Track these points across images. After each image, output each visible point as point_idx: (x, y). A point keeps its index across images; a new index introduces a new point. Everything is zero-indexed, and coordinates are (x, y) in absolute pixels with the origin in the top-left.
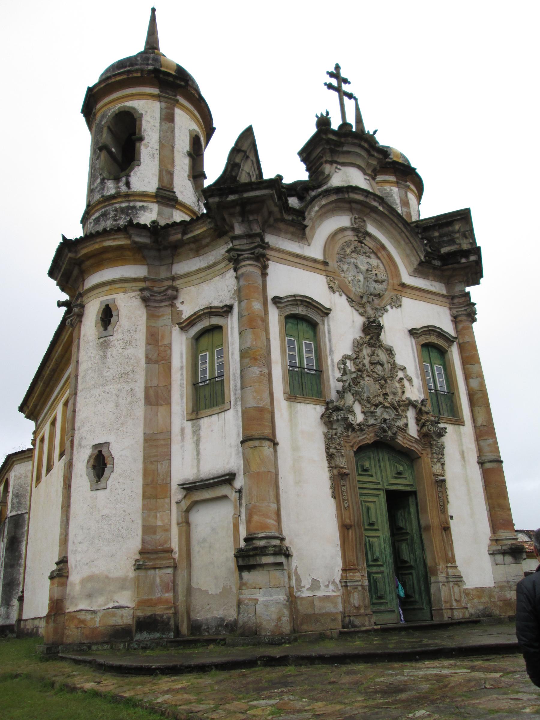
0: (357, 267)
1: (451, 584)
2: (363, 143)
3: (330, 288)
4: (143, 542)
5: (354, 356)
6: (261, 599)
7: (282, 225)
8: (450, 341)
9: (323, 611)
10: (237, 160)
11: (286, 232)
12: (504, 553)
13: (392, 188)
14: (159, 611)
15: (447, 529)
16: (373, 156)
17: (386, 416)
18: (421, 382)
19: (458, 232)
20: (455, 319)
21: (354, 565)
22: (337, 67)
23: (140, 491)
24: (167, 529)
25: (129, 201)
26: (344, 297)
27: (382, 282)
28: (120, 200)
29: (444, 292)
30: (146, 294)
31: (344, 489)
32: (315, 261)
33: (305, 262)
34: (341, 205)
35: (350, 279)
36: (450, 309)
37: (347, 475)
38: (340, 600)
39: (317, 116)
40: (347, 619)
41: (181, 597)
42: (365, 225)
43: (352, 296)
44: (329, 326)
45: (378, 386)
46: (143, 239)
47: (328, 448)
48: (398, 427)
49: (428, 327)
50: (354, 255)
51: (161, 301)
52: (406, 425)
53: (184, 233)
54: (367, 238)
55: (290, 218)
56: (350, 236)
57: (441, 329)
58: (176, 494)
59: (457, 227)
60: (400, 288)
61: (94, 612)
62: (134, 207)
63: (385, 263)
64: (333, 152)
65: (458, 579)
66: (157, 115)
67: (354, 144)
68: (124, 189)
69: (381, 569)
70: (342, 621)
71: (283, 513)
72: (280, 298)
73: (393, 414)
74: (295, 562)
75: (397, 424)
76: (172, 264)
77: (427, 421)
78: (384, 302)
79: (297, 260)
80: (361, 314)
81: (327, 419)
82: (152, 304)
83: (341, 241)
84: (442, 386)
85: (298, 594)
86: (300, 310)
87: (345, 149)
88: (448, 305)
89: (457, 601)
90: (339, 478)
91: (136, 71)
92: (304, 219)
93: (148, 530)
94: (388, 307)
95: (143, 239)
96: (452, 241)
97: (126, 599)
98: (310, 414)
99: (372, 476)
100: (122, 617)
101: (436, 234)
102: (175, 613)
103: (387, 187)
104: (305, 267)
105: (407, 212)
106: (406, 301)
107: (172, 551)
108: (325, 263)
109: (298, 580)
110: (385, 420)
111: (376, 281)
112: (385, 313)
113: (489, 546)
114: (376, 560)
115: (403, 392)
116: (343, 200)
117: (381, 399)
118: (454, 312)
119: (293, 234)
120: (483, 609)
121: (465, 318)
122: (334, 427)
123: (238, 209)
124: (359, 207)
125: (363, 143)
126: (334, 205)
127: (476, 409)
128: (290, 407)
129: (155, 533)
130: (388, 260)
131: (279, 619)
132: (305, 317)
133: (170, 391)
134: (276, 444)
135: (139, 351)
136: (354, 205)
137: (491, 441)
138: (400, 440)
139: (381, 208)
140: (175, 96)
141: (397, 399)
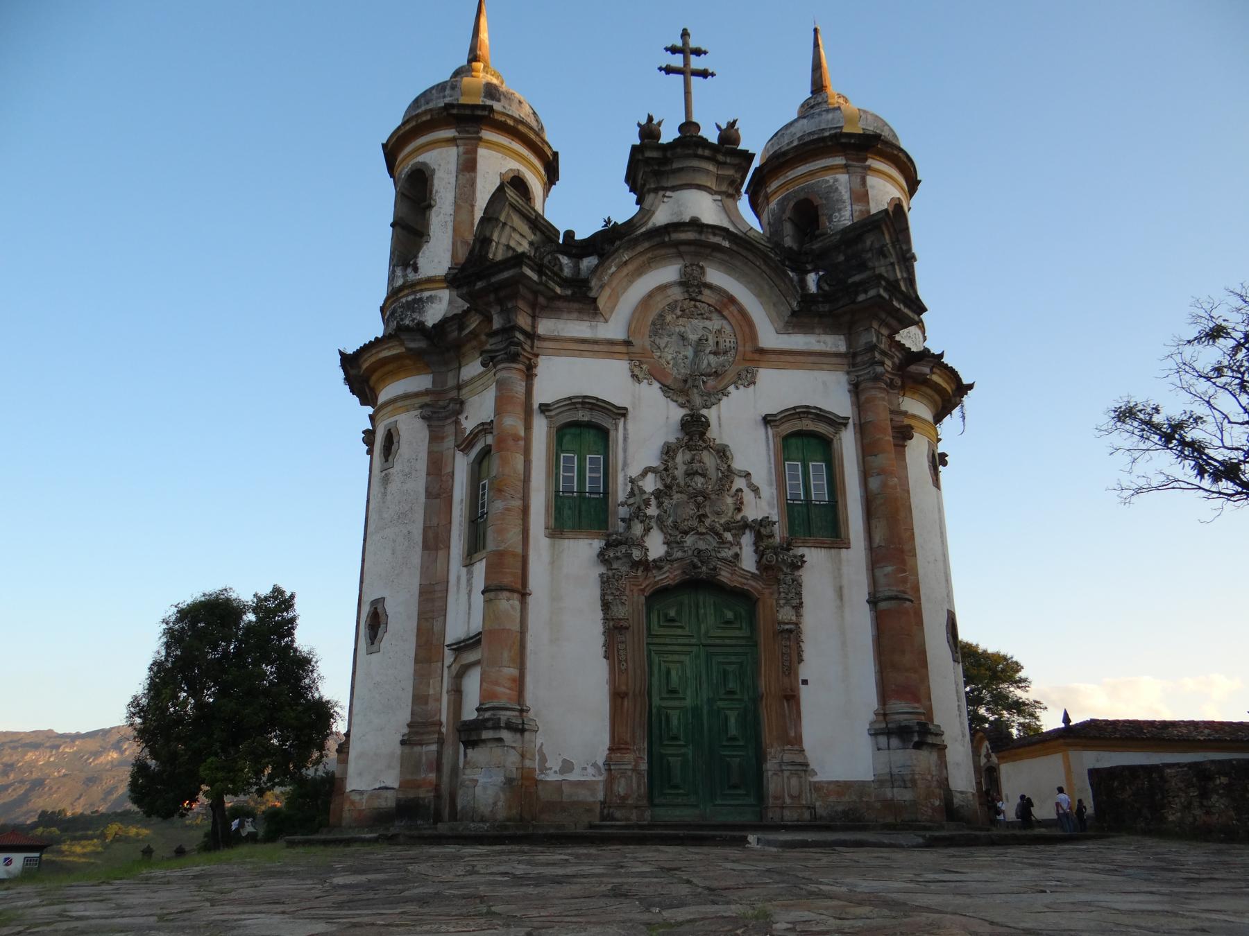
0: (683, 337)
1: (786, 774)
2: (700, 152)
3: (634, 376)
4: (413, 714)
5: (662, 467)
6: (482, 780)
7: (560, 304)
8: (838, 423)
9: (576, 799)
10: (488, 234)
11: (570, 312)
12: (888, 733)
13: (838, 176)
14: (422, 793)
15: (791, 698)
16: (725, 163)
17: (702, 545)
18: (775, 492)
19: (871, 249)
20: (856, 389)
21: (626, 743)
22: (685, 34)
23: (413, 655)
24: (439, 700)
25: (415, 293)
26: (656, 385)
27: (725, 353)
28: (406, 292)
29: (843, 348)
30: (427, 411)
31: (622, 646)
32: (611, 343)
33: (596, 347)
34: (663, 252)
35: (670, 357)
36: (848, 373)
37: (627, 628)
38: (601, 787)
39: (639, 125)
40: (606, 811)
41: (445, 779)
42: (703, 273)
43: (669, 382)
44: (625, 429)
45: (692, 506)
46: (419, 344)
47: (603, 595)
48: (723, 560)
49: (794, 408)
50: (681, 321)
51: (446, 418)
52: (737, 556)
53: (461, 328)
54: (707, 292)
55: (569, 292)
56: (677, 294)
57: (820, 409)
58: (449, 657)
59: (868, 243)
60: (757, 356)
61: (361, 793)
62: (421, 299)
63: (733, 322)
64: (658, 174)
65: (804, 767)
66: (453, 167)
67: (688, 157)
68: (411, 276)
69: (683, 750)
70: (602, 812)
71: (529, 679)
72: (547, 405)
73: (713, 541)
75: (723, 554)
76: (460, 368)
77: (767, 548)
78: (725, 381)
79: (583, 347)
80: (682, 406)
81: (602, 557)
82: (436, 423)
83: (660, 303)
84: (820, 493)
85: (542, 777)
86: (583, 416)
87: (675, 165)
88: (846, 368)
89: (791, 797)
90: (614, 631)
91: (426, 112)
92: (590, 289)
93: (419, 699)
94: (731, 389)
95: (419, 344)
96: (863, 266)
97: (392, 779)
98: (582, 552)
99: (681, 627)
100: (386, 798)
101: (841, 258)
102: (438, 797)
103: (829, 178)
104: (596, 354)
105: (861, 211)
107: (441, 724)
108: (627, 343)
109: (543, 759)
110: (699, 551)
111: (715, 353)
112: (725, 398)
113: (871, 723)
114: (675, 738)
115: (739, 510)
116: (663, 245)
117: (695, 523)
118: (853, 378)
119: (580, 311)
120: (844, 811)
121: (870, 384)
122: (615, 566)
123: (492, 297)
124: (692, 248)
125: (700, 152)
126: (650, 255)
127: (874, 522)
128: (553, 546)
129: (426, 703)
130: (739, 317)
131: (495, 804)
132: (588, 425)
133: (449, 531)
134: (524, 595)
135: (419, 484)
136: (682, 248)
137: (889, 569)
138: (725, 576)
139: (726, 244)
140: (478, 132)
141: (722, 521)
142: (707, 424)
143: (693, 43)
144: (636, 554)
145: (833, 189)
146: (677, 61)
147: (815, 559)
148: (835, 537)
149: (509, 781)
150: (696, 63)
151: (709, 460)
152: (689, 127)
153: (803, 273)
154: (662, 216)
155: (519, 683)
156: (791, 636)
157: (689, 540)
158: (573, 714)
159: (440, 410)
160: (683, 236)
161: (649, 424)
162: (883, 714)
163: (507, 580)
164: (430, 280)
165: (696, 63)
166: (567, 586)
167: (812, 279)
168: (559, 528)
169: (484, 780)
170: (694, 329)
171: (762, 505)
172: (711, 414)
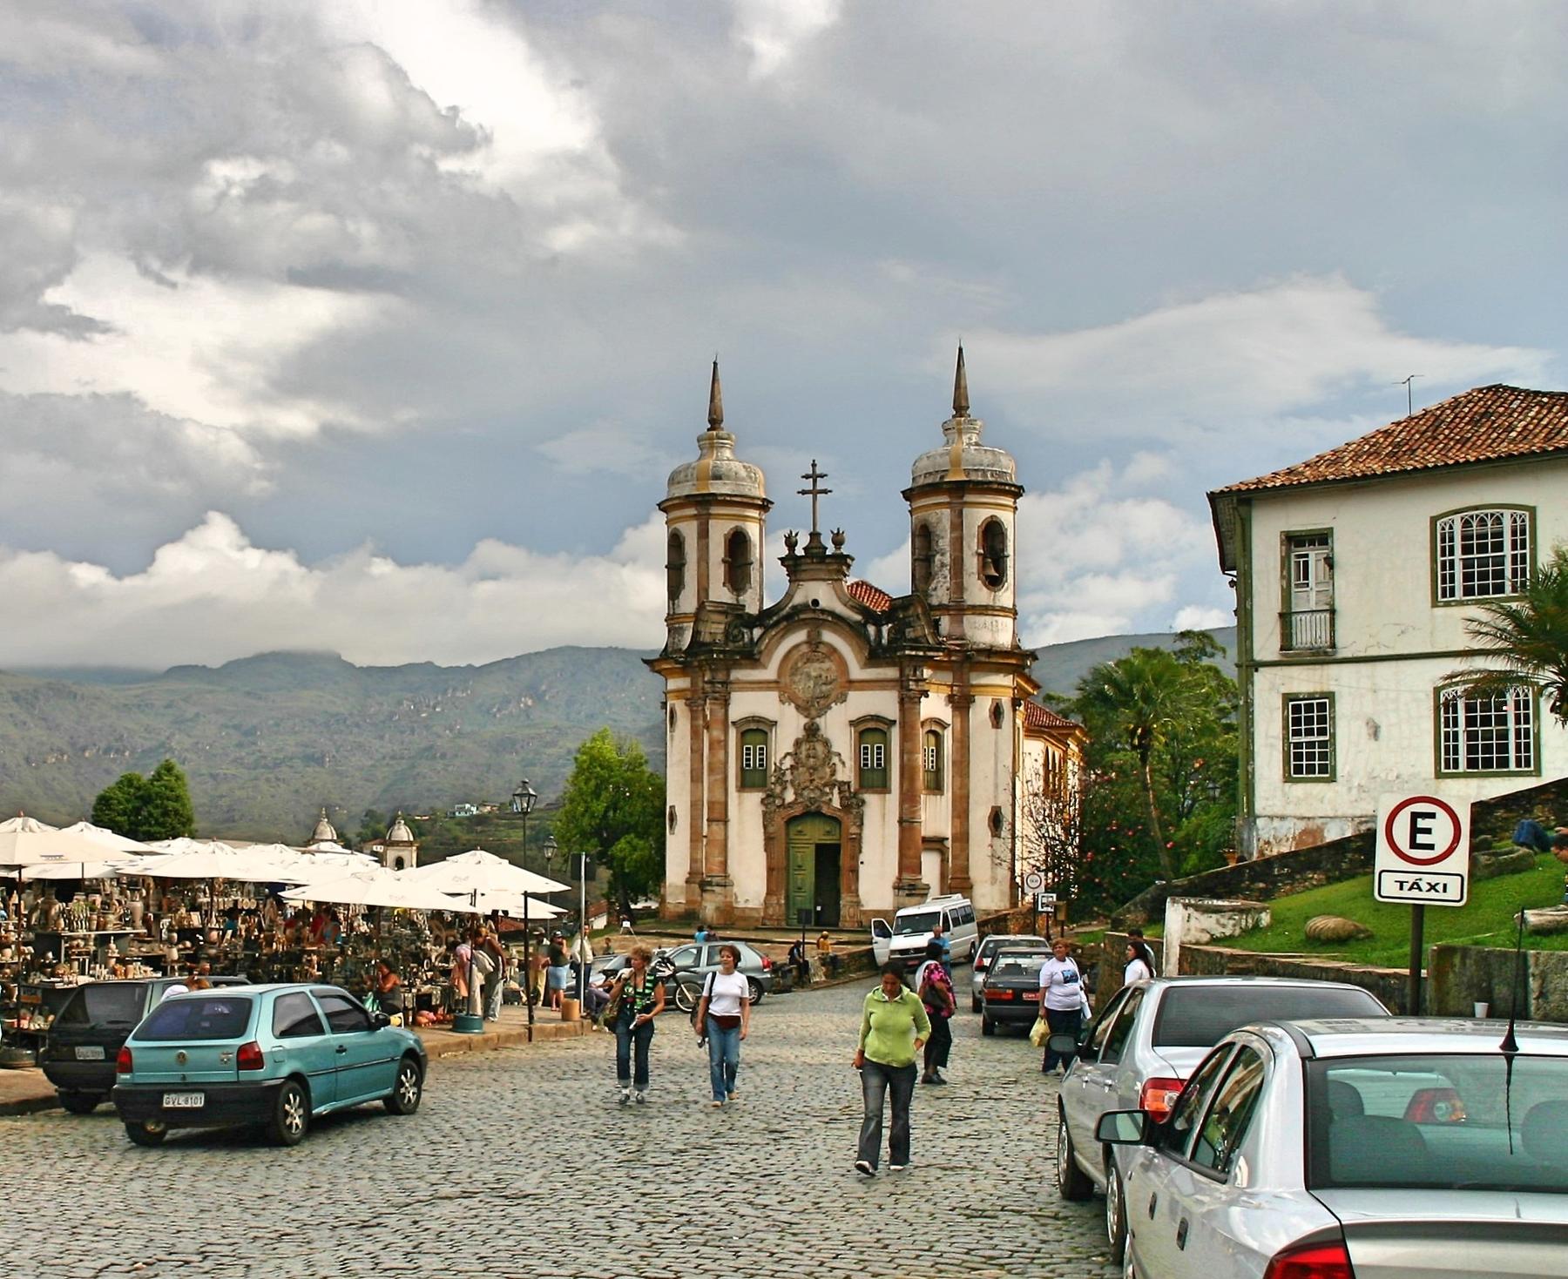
0: (809, 675)
20: (902, 702)
22: (814, 465)
32: (769, 682)
56: (805, 649)
65: (858, 903)
74: (735, 889)
86: (753, 726)
90: (769, 840)
93: (693, 861)
104: (761, 689)
106: (852, 695)
108: (776, 682)
132: (757, 730)
134: (726, 822)
138: (825, 810)
142: (818, 729)
143: (818, 472)
144: (778, 802)
145: (939, 521)
146: (808, 484)
147: (872, 800)
148: (884, 788)
149: (717, 909)
150: (821, 484)
151: (820, 748)
152: (815, 535)
153: (878, 626)
154: (798, 599)
155: (725, 864)
156: (857, 841)
157: (806, 793)
158: (750, 881)
159: (694, 701)
160: (803, 616)
161: (789, 727)
162: (900, 879)
163: (716, 815)
164: (686, 615)
165: (821, 484)
166: (746, 816)
167: (885, 629)
168: (743, 786)
169: (709, 908)
170: (814, 669)
171: (846, 773)
172: (820, 721)
